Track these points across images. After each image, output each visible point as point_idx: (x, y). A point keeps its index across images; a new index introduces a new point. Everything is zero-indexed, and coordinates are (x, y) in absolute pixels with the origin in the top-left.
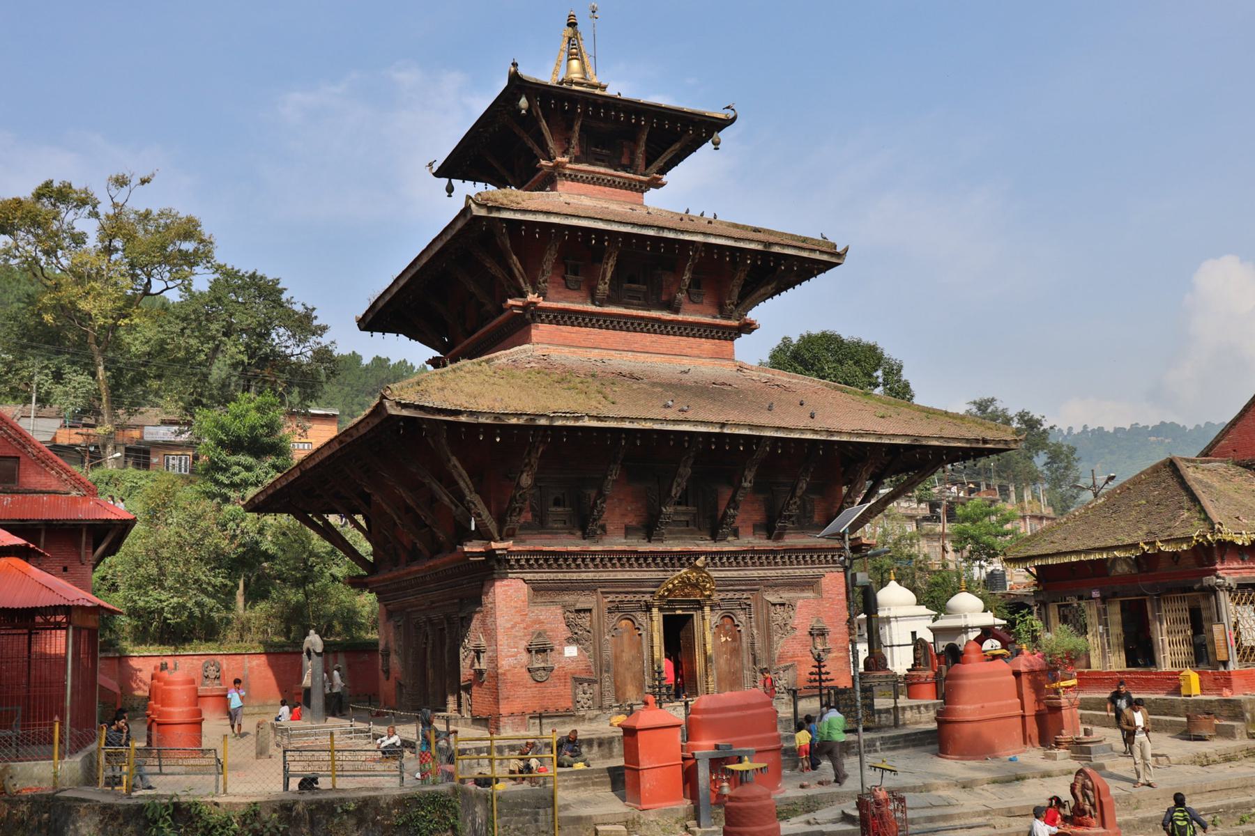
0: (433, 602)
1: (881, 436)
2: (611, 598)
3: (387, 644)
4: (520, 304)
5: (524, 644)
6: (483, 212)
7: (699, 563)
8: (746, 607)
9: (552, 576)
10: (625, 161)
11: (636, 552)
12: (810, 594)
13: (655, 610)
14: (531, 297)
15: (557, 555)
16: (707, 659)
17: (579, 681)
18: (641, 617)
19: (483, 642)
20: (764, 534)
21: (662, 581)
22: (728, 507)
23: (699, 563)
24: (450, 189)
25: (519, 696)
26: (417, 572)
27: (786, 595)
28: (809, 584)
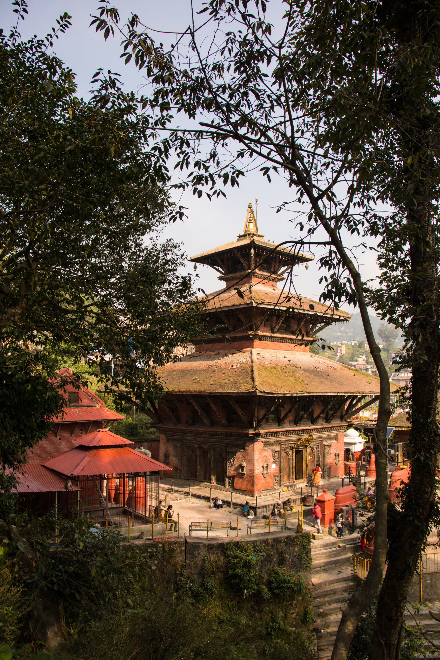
3: (167, 452)
5: (261, 465)
6: (255, 305)
8: (317, 447)
10: (272, 270)
11: (294, 431)
12: (334, 441)
14: (259, 332)
16: (307, 466)
17: (275, 476)
18: (290, 453)
19: (245, 463)
20: (324, 421)
22: (320, 413)
24: (195, 268)
25: (259, 483)
27: (329, 442)
28: (336, 438)
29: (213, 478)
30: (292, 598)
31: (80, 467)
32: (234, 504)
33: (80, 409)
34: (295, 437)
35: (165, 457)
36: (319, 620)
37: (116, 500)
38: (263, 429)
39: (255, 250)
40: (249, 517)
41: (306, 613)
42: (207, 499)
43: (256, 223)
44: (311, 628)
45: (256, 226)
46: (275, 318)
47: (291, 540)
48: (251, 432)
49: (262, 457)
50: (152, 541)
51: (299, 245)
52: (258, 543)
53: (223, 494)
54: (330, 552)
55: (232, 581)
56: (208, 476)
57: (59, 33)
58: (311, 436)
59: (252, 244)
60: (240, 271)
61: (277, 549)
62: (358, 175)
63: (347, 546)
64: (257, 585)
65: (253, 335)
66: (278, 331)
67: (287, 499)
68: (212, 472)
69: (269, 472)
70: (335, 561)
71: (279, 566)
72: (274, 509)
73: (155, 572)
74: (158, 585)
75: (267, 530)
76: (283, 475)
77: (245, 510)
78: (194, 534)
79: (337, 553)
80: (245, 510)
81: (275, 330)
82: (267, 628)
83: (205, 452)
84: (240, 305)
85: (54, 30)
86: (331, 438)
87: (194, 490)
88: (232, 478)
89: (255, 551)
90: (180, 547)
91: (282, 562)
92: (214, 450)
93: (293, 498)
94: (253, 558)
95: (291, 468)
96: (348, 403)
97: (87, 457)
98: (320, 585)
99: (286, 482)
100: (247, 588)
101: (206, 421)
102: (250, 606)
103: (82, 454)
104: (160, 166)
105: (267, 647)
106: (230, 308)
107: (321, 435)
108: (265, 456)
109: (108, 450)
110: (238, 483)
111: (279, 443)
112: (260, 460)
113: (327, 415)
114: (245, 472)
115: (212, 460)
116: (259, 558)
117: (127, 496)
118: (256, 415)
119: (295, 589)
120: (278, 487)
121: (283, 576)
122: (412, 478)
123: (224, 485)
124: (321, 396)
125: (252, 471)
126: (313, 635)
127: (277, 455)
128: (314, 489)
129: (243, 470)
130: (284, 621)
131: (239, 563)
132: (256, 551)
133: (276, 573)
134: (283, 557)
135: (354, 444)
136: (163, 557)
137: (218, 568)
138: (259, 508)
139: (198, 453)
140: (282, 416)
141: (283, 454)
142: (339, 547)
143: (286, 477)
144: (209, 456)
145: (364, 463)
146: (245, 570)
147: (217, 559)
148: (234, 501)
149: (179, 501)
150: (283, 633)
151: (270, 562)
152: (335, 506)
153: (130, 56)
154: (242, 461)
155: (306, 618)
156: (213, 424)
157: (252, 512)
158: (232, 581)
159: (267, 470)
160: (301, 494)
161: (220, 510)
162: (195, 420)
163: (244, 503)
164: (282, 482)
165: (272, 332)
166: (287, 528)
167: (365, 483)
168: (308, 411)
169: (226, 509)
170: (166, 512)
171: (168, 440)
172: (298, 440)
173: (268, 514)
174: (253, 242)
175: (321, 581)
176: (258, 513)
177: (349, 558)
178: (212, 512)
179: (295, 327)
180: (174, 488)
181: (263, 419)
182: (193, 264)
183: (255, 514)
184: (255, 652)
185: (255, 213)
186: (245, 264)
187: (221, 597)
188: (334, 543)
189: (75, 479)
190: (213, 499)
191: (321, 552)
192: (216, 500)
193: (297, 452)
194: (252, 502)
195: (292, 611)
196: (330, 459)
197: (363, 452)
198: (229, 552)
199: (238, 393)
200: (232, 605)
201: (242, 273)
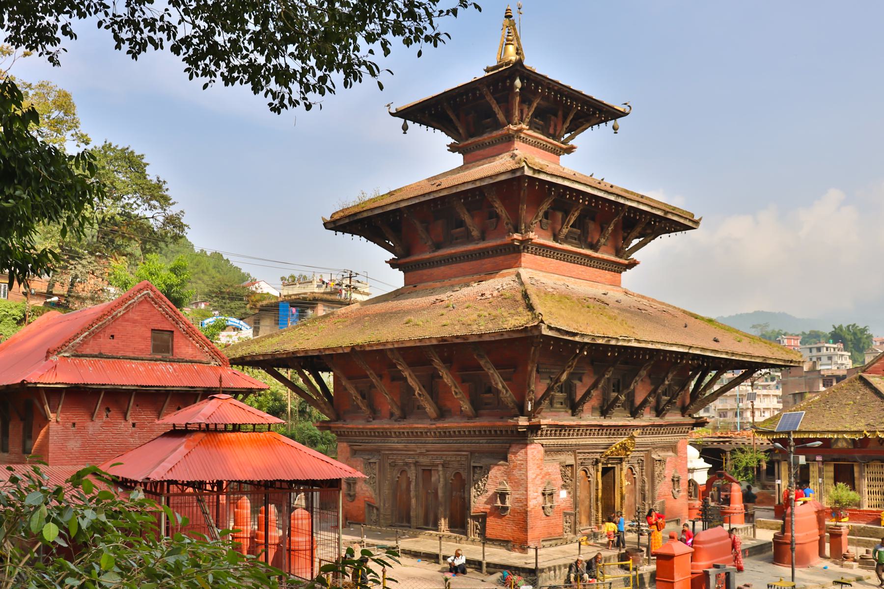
0: (428, 451)
1: (752, 357)
4: (520, 238)
6: (528, 172)
7: (635, 433)
8: (641, 462)
11: (601, 426)
13: (600, 465)
14: (531, 235)
16: (622, 498)
18: (592, 471)
21: (610, 445)
22: (649, 395)
23: (635, 433)
26: (417, 428)
29: (443, 524)
34: (603, 440)
56: (431, 518)
65: (521, 242)
66: (565, 240)
68: (441, 509)
81: (562, 236)
83: (427, 472)
84: (497, 175)
87: (405, 544)
92: (443, 466)
101: (430, 409)
106: (478, 184)
107: (649, 439)
113: (658, 402)
115: (441, 485)
139: (412, 473)
140: (578, 398)
144: (433, 479)
156: (442, 414)
162: (408, 409)
172: (608, 447)
193: (605, 471)
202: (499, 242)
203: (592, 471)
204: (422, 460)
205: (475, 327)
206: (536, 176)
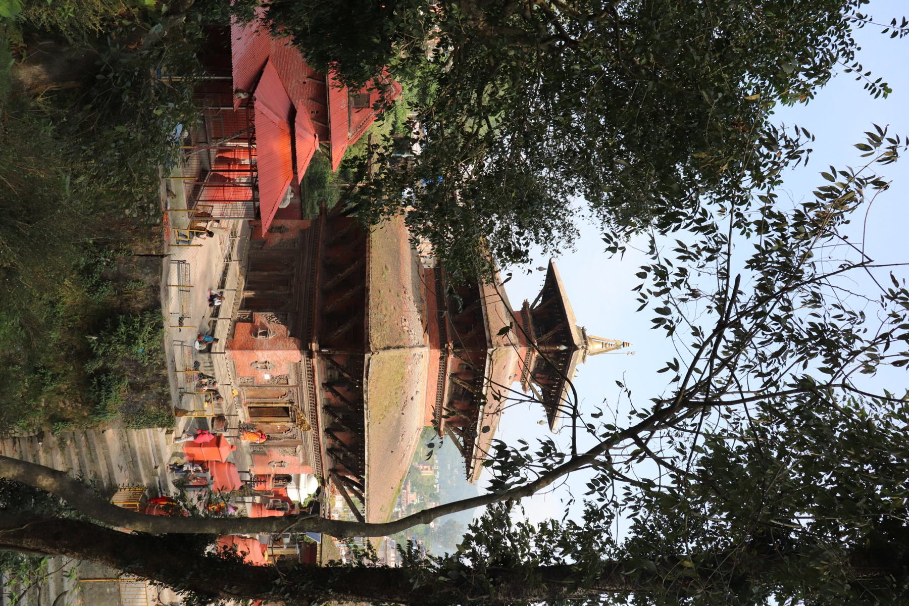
2: (295, 390)
3: (287, 230)
5: (269, 360)
6: (490, 351)
8: (294, 437)
9: (303, 371)
10: (537, 375)
11: (316, 405)
12: (302, 461)
13: (289, 405)
14: (451, 357)
15: (313, 376)
16: (267, 423)
18: (286, 399)
19: (271, 337)
20: (329, 447)
22: (340, 441)
24: (540, 269)
27: (301, 454)
28: (306, 463)
29: (250, 294)
30: (86, 402)
31: (266, 111)
32: (215, 322)
33: (346, 110)
34: (307, 407)
35: (280, 228)
36: (55, 439)
37: (221, 160)
38: (319, 362)
39: (565, 351)
40: (197, 343)
41: (65, 421)
42: (222, 285)
43: (602, 352)
44: (44, 429)
45: (598, 353)
46: (471, 378)
47: (165, 400)
48: (314, 346)
49: (280, 361)
50: (164, 209)
51: (571, 411)
52: (161, 356)
53: (229, 306)
54: (149, 454)
55: (109, 320)
57: (863, 81)
58: (309, 428)
59: (572, 347)
60: (536, 332)
61: (153, 382)
62: (668, 493)
63: (157, 479)
64: (104, 354)
65: (447, 349)
66: (453, 383)
67: (222, 396)
69: (260, 371)
70: (136, 461)
71: (130, 384)
72: (208, 377)
73: (121, 213)
74: (103, 218)
75: (179, 367)
76: (255, 390)
77: (207, 339)
78: (174, 267)
79: (147, 464)
80: (207, 339)
81: (455, 379)
82: (44, 368)
85: (868, 74)
86: (305, 455)
87: (235, 267)
88: (250, 320)
89: (150, 351)
90: (156, 247)
91: (135, 388)
93: (224, 403)
94: (140, 348)
95: (264, 400)
96: (354, 479)
97: (280, 120)
98: (103, 440)
99: (246, 393)
100: (100, 341)
102: (75, 344)
103: (284, 113)
104: (680, 220)
105: (17, 368)
106: (485, 317)
107: (310, 442)
108: (281, 365)
109: (289, 149)
110: (244, 328)
111: (299, 385)
112: (275, 358)
114: (259, 337)
116: (140, 356)
117: (226, 175)
118: (337, 353)
119: (98, 407)
120: (238, 383)
121: (116, 390)
122: (250, 567)
123: (241, 308)
124: (364, 442)
125: (260, 348)
126: (34, 432)
127: (282, 381)
128: (235, 433)
129: (261, 334)
130: (53, 391)
131: (134, 329)
132: (150, 353)
133: (120, 381)
134: (142, 389)
135: (298, 488)
136: (142, 224)
137: (126, 300)
138: (210, 357)
140: (335, 388)
141: (284, 390)
142: (156, 467)
143: (252, 393)
145: (271, 501)
146: (124, 337)
147: (139, 299)
148: (219, 322)
149: (219, 246)
150: (37, 389)
151: (135, 372)
152: (212, 462)
153: (832, 180)
154: (274, 332)
155: (58, 421)
156: (326, 293)
157: (204, 347)
158: (109, 320)
159: (261, 368)
160: (229, 415)
161: (207, 304)
163: (217, 336)
164: (245, 388)
165: (452, 375)
166: (181, 395)
167: (244, 502)
168: (344, 424)
169: (209, 311)
170: (205, 229)
171: (303, 232)
172: (303, 410)
173: (202, 369)
174: (576, 348)
175: (109, 442)
176: (202, 355)
177: (141, 481)
178: (204, 292)
179: (458, 407)
180: (237, 240)
181: (332, 361)
182: (546, 266)
183: (201, 351)
184: (12, 351)
185: (616, 351)
186: (545, 337)
187: (86, 304)
188: (161, 460)
189: (249, 103)
190: (222, 293)
191: (149, 442)
192: (221, 297)
193: (286, 409)
194: (217, 347)
195: (67, 402)
196: (276, 454)
197: (287, 499)
198: (148, 315)
199: (368, 328)
200: (76, 320)
201: (533, 333)
202: (448, 333)
203: (286, 399)
204: (294, 281)
205: (375, 311)
206: (488, 357)
